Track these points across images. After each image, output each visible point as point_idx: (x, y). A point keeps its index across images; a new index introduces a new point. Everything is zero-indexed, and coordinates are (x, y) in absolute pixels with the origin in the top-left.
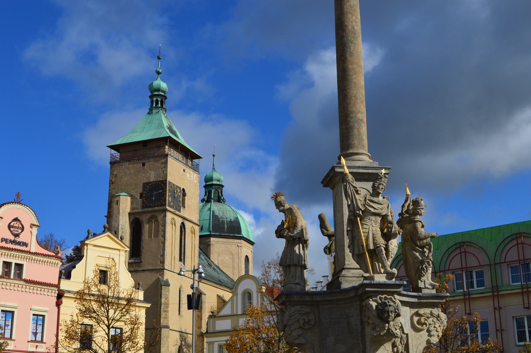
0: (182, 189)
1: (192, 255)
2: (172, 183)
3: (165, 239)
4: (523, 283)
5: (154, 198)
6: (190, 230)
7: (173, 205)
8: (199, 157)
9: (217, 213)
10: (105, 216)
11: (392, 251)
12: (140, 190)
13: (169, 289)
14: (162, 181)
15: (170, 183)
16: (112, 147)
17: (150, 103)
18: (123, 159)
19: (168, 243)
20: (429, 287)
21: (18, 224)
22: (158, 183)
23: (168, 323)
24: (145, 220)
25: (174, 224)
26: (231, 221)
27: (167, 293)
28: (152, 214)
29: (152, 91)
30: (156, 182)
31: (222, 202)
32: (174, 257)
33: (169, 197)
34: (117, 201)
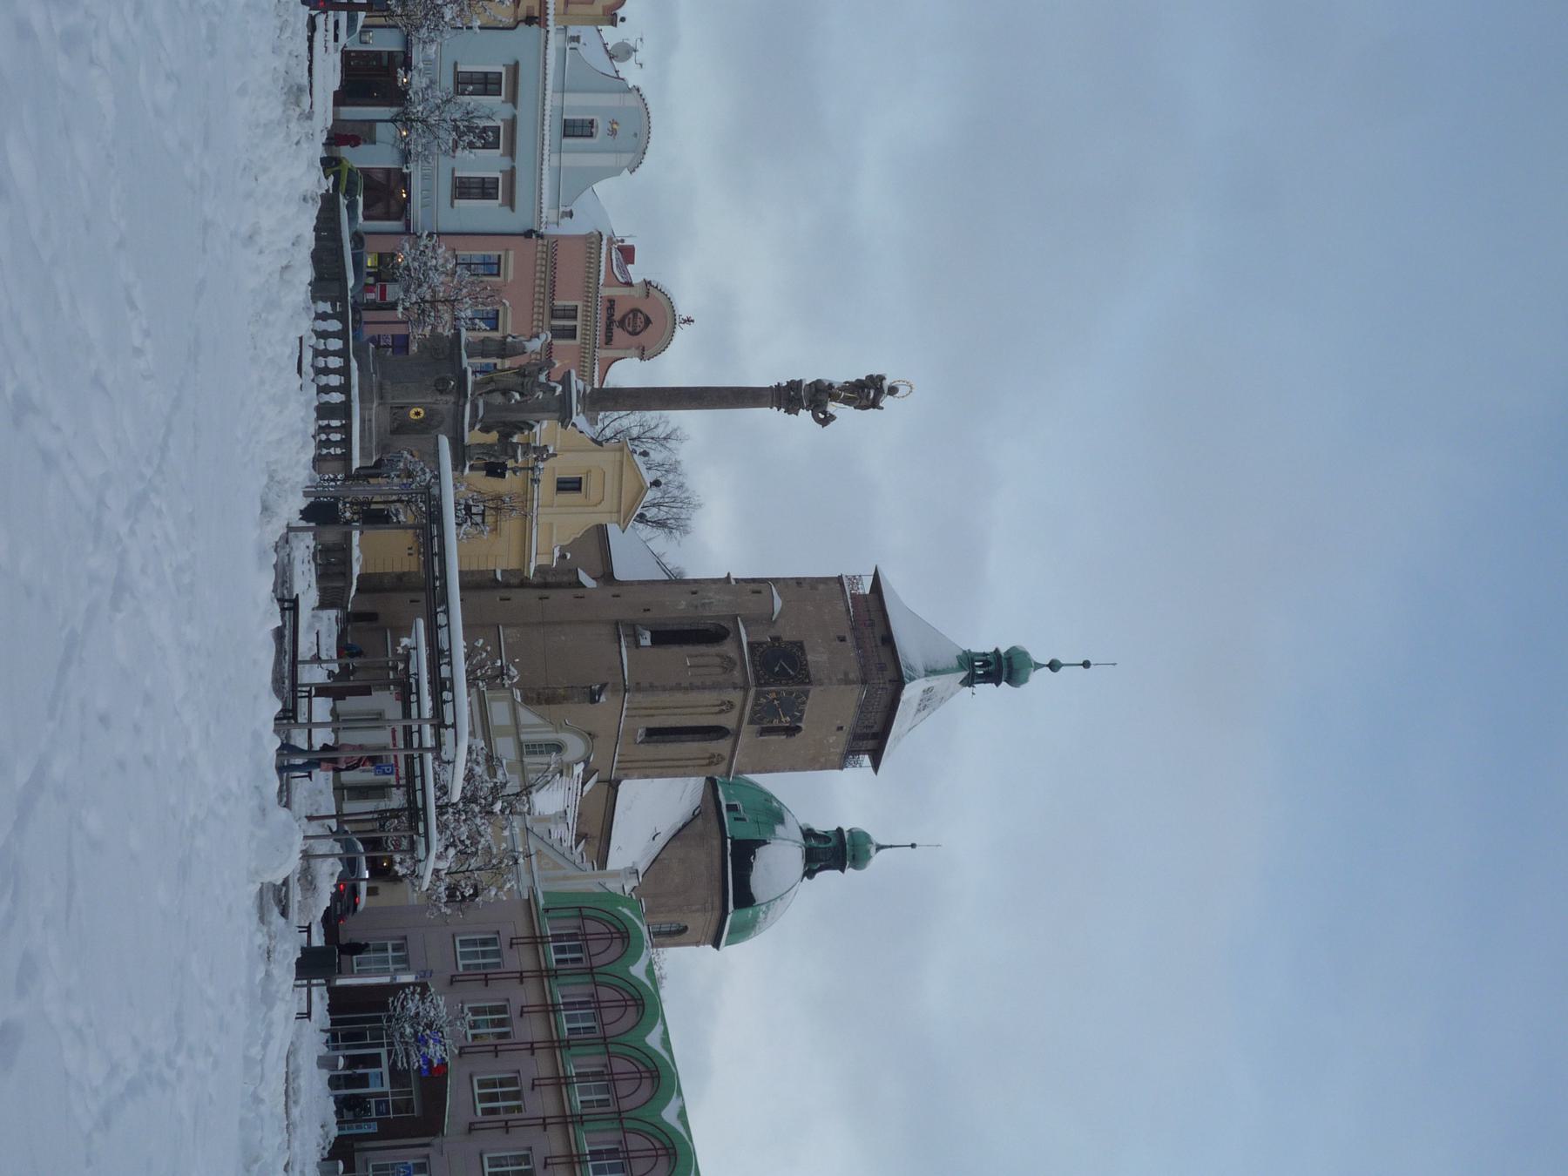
0: (799, 724)
3: (686, 689)
4: (576, 1085)
7: (760, 705)
8: (876, 765)
10: (729, 574)
13: (584, 702)
14: (808, 676)
15: (806, 694)
17: (982, 651)
19: (679, 698)
21: (642, 326)
22: (805, 670)
24: (725, 648)
27: (576, 700)
28: (739, 663)
29: (1007, 652)
30: (806, 665)
31: (805, 867)
32: (653, 716)
34: (759, 592)
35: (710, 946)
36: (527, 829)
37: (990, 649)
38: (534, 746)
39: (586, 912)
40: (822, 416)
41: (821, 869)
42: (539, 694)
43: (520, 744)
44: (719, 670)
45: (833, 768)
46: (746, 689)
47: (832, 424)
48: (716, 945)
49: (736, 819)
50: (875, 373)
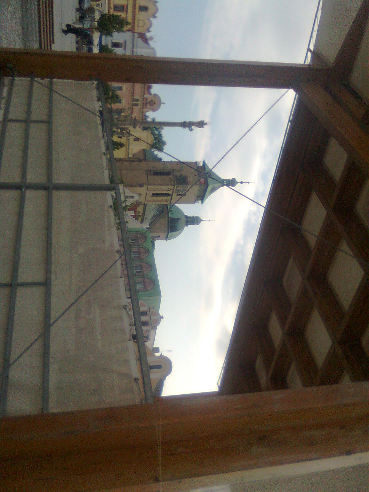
3: (162, 185)
8: (202, 203)
16: (204, 163)
19: (160, 187)
25: (169, 190)
35: (165, 240)
39: (138, 233)
40: (191, 129)
41: (189, 225)
46: (174, 186)
47: (192, 132)
48: (166, 240)
50: (202, 120)
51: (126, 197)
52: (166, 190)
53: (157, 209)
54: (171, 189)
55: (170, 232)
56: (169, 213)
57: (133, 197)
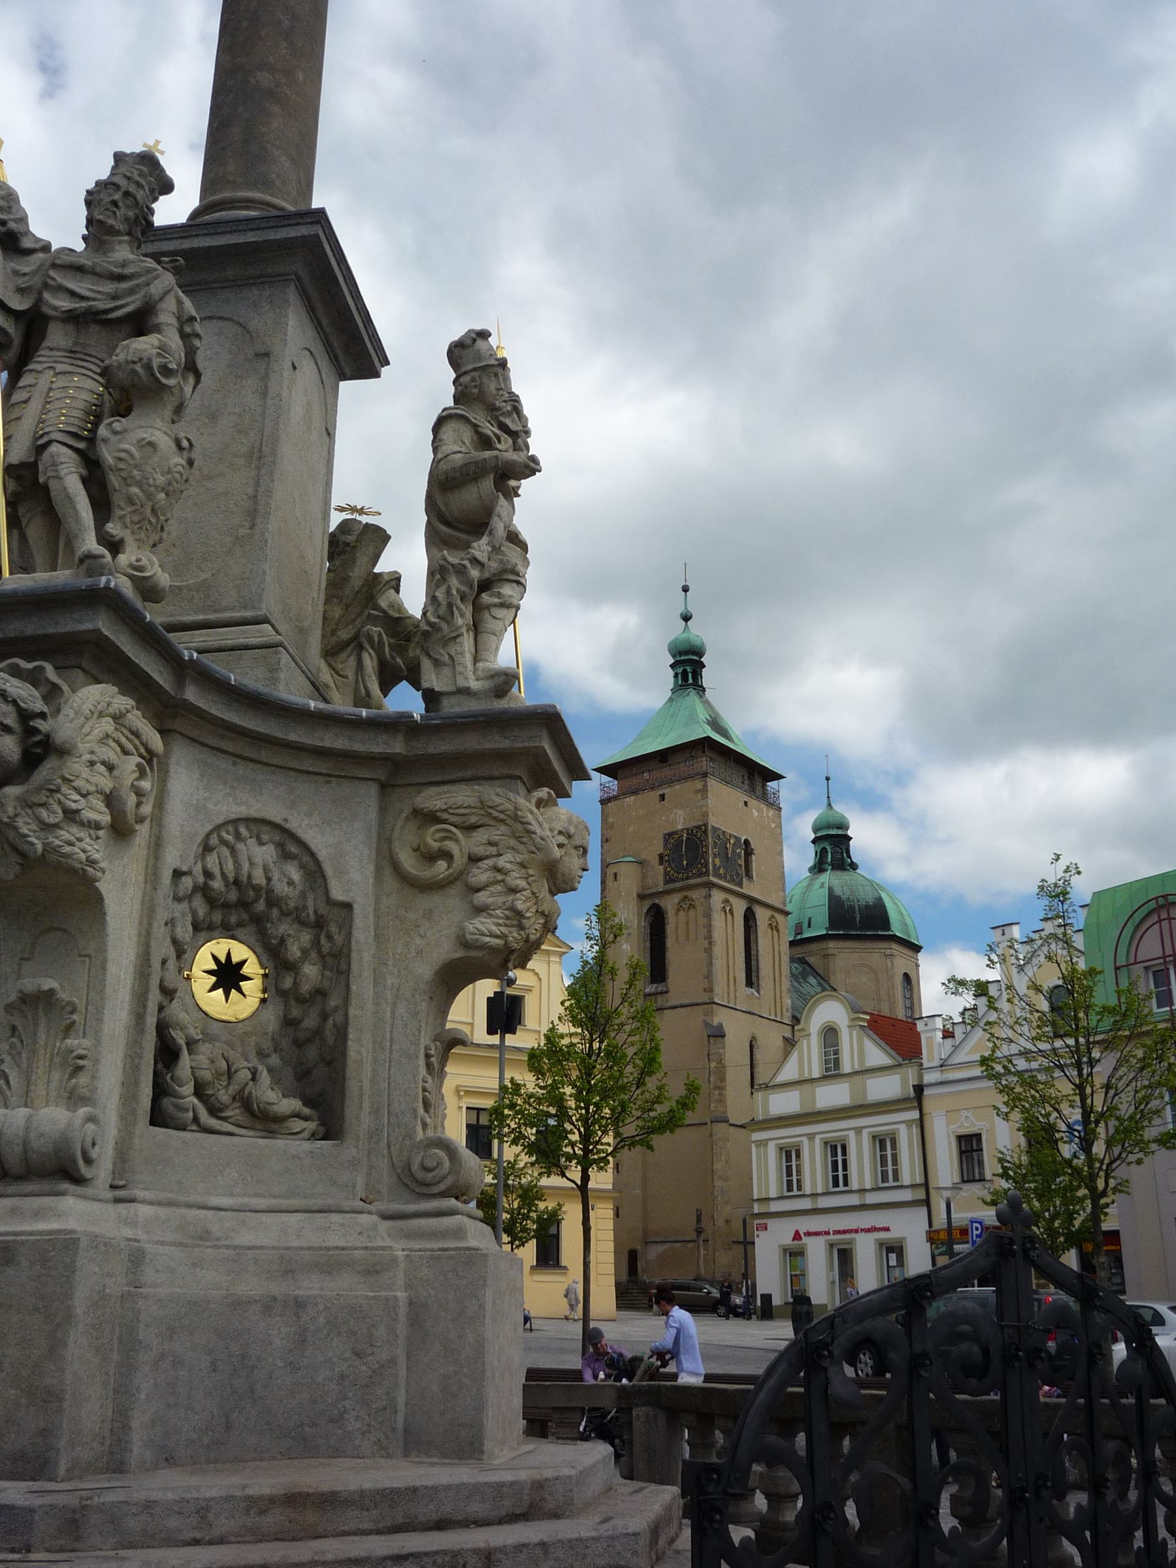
1: (774, 973)
2: (719, 829)
3: (710, 943)
5: (685, 862)
6: (767, 923)
8: (778, 777)
9: (838, 891)
11: (122, 465)
12: (659, 848)
13: (724, 1043)
14: (699, 827)
15: (715, 829)
18: (623, 793)
19: (718, 950)
20: (475, 685)
23: (725, 1112)
25: (729, 911)
26: (867, 906)
28: (683, 894)
29: (674, 656)
30: (688, 829)
33: (715, 856)
34: (616, 874)
35: (919, 954)
36: (941, 1066)
37: (671, 673)
38: (826, 1062)
39: (1122, 961)
41: (849, 857)
42: (716, 1088)
43: (824, 1078)
44: (692, 912)
45: (780, 817)
48: (917, 949)
49: (809, 926)
51: (832, 1071)
52: (730, 927)
53: (799, 983)
54: (727, 901)
55: (889, 929)
56: (806, 935)
57: (830, 1033)
